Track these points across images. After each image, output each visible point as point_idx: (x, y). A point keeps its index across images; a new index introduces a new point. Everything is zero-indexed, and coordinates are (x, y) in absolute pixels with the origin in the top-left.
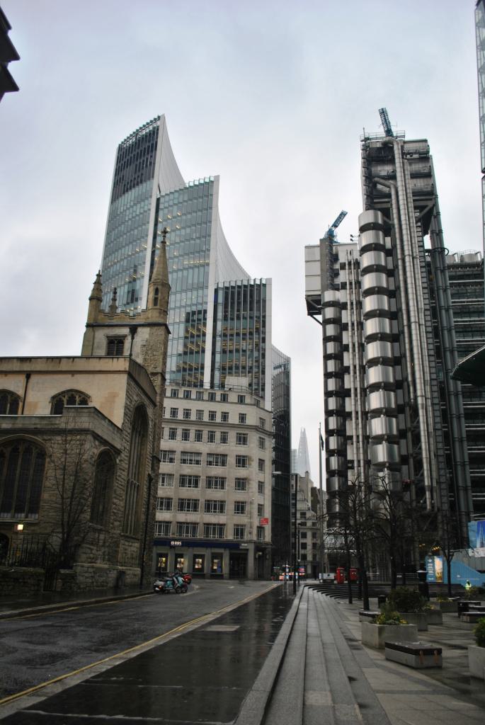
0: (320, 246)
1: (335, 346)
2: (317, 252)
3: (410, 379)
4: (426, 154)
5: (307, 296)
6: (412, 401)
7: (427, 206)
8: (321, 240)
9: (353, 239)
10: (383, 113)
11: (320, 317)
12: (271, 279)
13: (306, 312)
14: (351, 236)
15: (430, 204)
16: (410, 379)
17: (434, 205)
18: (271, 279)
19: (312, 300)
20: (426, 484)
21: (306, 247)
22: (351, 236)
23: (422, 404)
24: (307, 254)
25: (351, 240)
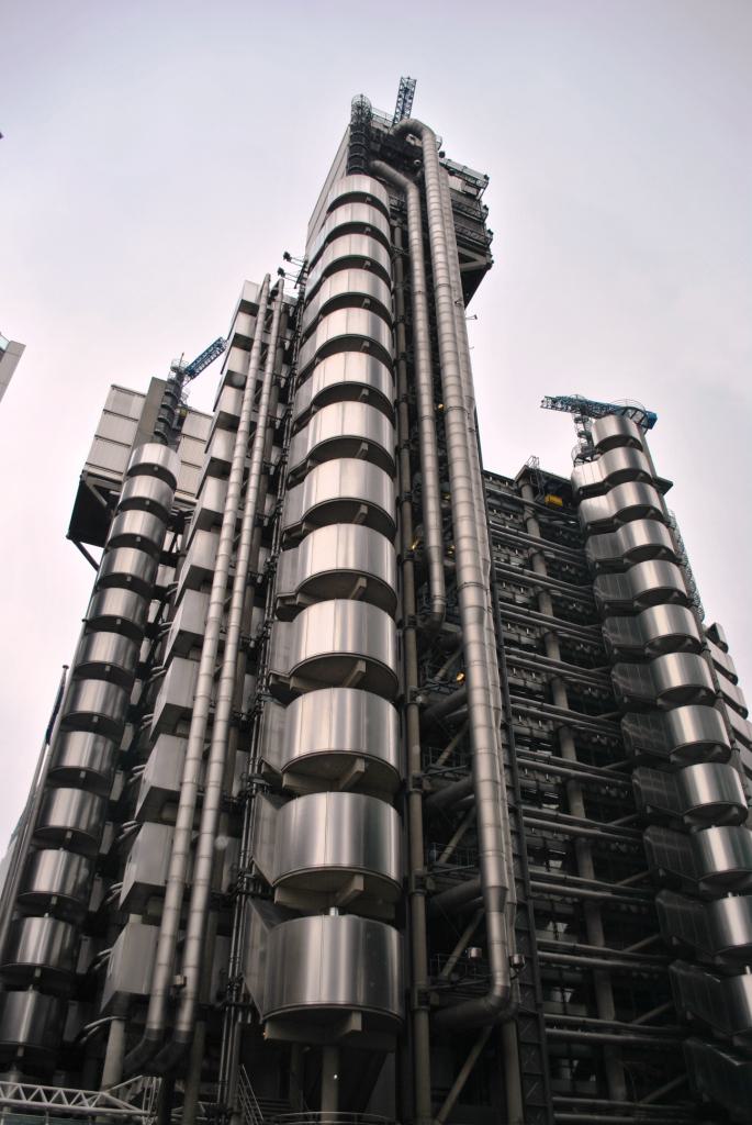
1: (140, 558)
3: (434, 539)
4: (479, 188)
5: (86, 475)
7: (475, 260)
8: (154, 380)
9: (288, 267)
10: (406, 92)
11: (97, 552)
12: (22, 347)
13: (66, 531)
14: (287, 257)
15: (481, 261)
16: (434, 539)
17: (489, 266)
18: (22, 347)
19: (96, 486)
20: (492, 878)
21: (114, 387)
22: (287, 257)
23: (481, 609)
24: (115, 400)
25: (281, 272)
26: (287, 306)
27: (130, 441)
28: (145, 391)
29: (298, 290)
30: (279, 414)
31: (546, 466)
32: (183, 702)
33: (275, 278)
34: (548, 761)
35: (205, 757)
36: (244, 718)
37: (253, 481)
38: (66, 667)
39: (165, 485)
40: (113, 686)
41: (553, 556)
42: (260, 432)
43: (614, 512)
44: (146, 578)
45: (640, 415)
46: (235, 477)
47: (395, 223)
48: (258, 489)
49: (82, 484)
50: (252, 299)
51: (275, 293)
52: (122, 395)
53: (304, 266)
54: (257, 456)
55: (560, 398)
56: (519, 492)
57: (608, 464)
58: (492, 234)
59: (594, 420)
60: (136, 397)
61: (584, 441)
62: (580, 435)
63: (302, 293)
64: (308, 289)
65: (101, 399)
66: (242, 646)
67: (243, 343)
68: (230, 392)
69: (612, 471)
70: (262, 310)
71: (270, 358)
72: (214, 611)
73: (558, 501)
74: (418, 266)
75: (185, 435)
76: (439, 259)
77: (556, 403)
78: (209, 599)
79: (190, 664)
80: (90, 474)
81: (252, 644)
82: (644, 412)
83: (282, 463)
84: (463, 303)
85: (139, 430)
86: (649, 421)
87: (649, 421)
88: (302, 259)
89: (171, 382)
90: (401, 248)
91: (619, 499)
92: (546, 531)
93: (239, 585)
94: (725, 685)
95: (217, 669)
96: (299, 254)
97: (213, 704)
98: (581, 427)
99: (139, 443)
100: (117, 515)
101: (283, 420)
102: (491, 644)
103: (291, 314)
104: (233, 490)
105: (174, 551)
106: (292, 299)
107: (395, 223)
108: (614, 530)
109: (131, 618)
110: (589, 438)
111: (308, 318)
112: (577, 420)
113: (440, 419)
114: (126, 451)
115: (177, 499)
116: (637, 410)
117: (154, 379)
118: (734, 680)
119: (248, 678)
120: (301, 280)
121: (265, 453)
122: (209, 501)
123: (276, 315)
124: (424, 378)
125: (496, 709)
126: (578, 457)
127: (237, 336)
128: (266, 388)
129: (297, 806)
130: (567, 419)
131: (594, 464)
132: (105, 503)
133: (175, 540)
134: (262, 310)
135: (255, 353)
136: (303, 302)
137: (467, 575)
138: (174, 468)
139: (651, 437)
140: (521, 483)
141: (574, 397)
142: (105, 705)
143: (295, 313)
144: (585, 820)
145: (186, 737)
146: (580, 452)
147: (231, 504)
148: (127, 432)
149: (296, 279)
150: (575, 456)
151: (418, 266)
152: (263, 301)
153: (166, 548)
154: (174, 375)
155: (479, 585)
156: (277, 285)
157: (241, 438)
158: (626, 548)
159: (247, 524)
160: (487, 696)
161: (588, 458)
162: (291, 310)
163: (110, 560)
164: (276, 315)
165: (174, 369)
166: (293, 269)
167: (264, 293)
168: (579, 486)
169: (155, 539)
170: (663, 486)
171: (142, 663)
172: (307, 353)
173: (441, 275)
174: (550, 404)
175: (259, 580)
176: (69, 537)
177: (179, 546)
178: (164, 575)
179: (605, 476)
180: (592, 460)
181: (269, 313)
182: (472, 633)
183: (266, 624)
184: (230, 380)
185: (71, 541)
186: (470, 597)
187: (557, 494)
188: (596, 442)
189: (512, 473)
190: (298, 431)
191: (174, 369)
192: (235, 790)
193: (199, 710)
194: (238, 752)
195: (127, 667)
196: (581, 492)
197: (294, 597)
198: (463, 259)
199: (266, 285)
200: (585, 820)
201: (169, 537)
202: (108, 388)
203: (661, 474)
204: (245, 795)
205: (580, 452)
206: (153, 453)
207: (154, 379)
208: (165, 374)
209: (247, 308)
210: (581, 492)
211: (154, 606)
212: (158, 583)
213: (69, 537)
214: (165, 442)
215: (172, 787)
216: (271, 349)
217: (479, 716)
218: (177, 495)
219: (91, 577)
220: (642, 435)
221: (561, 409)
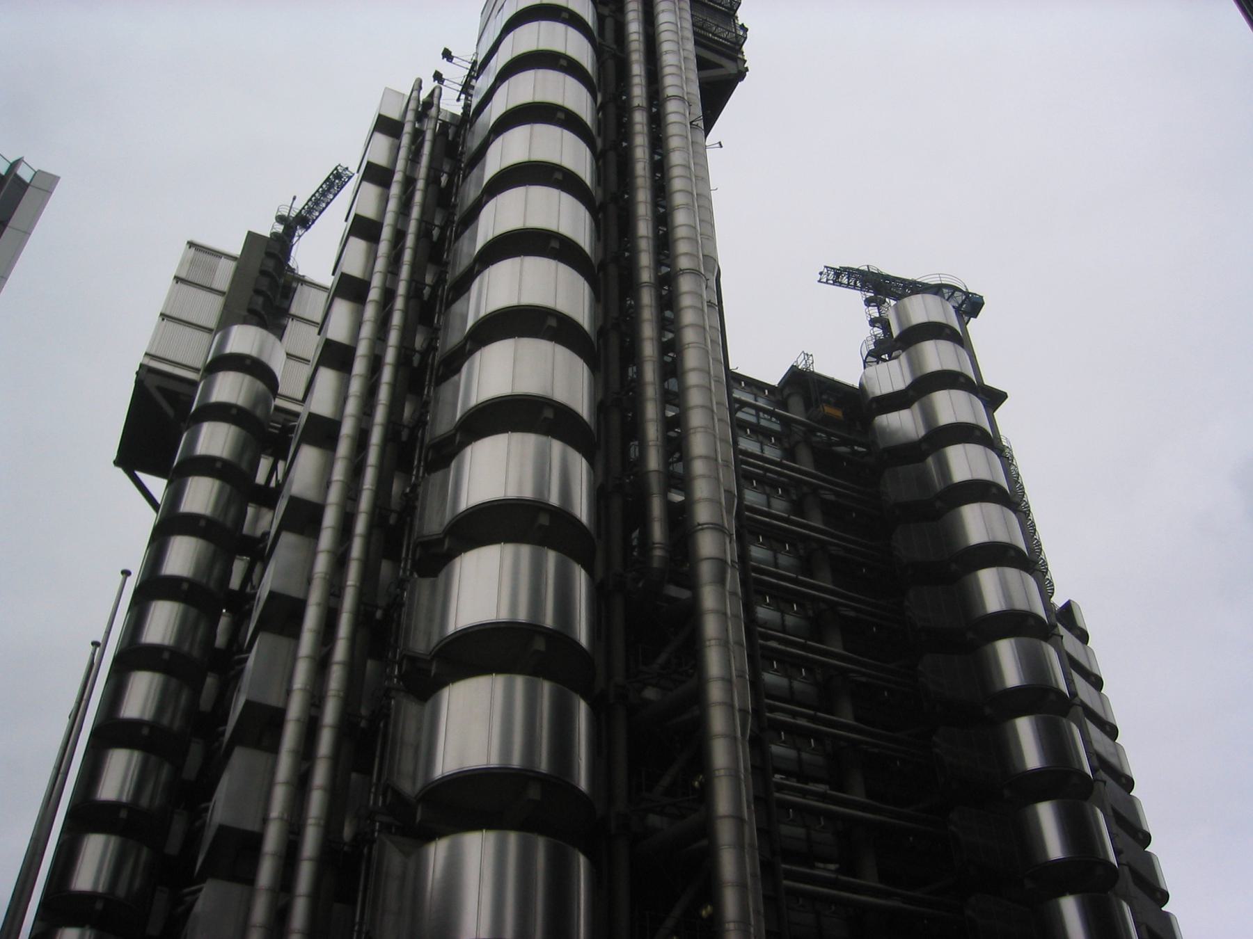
0: (242, 262)
2: (223, 275)
6: (658, 553)
7: (721, 66)
8: (252, 238)
11: (158, 486)
12: (54, 180)
13: (114, 455)
14: (447, 55)
15: (730, 68)
17: (741, 75)
18: (54, 180)
19: (159, 389)
21: (191, 244)
22: (447, 55)
23: (721, 563)
25: (438, 77)
26: (445, 125)
27: (212, 323)
28: (237, 250)
29: (462, 103)
30: (429, 279)
31: (825, 367)
32: (273, 700)
33: (429, 85)
34: (823, 797)
35: (301, 783)
36: (363, 724)
37: (387, 375)
38: (95, 644)
39: (260, 386)
40: (174, 682)
41: (832, 498)
42: (399, 303)
43: (922, 432)
44: (229, 524)
45: (959, 297)
46: (359, 367)
47: (606, 11)
48: (394, 385)
49: (139, 383)
50: (395, 114)
51: (428, 104)
52: (208, 258)
53: (472, 68)
54: (393, 337)
55: (845, 269)
56: (784, 405)
57: (914, 364)
58: (746, 30)
59: (893, 303)
60: (223, 261)
61: (878, 331)
62: (873, 322)
63: (467, 107)
64: (475, 101)
65: (173, 259)
66: (362, 617)
67: (376, 174)
68: (358, 246)
69: (919, 374)
70: (408, 128)
71: (418, 197)
72: (322, 564)
73: (838, 413)
74: (637, 69)
75: (294, 317)
76: (669, 60)
77: (841, 276)
78: (316, 544)
79: (284, 642)
80: (151, 370)
81: (379, 614)
82: (967, 294)
83: (431, 348)
84: (701, 124)
85: (226, 307)
86: (971, 306)
87: (971, 306)
88: (469, 59)
89: (275, 235)
90: (614, 46)
91: (928, 415)
92: (823, 458)
93: (360, 526)
94: (1084, 690)
95: (325, 650)
96: (467, 50)
97: (316, 700)
98: (874, 312)
99: (226, 321)
100: (188, 428)
101: (434, 288)
102: (736, 616)
103: (450, 138)
104: (356, 386)
105: (273, 484)
106: (453, 115)
107: (606, 11)
108: (922, 458)
109: (204, 581)
110: (885, 325)
111: (474, 143)
112: (868, 302)
113: (667, 284)
114: (206, 336)
115: (278, 409)
116: (955, 289)
117: (250, 234)
118: (1097, 683)
119: (370, 665)
120: (467, 88)
121: (407, 333)
122: (322, 403)
123: (429, 136)
124: (644, 228)
125: (743, 711)
126: (870, 354)
127: (369, 165)
128: (410, 241)
129: (438, 852)
130: (855, 298)
131: (895, 362)
132: (170, 412)
133: (274, 469)
134: (408, 128)
135: (395, 190)
136: (469, 118)
137: (703, 514)
138: (278, 364)
139: (975, 327)
140: (787, 392)
141: (865, 268)
142: (160, 708)
143: (457, 134)
144: (880, 886)
145: (274, 749)
146: (872, 347)
147: (352, 407)
148: (208, 309)
149: (460, 88)
150: (865, 354)
151: (637, 69)
152: (410, 116)
153: (260, 478)
154: (280, 228)
155: (718, 528)
156: (432, 95)
157: (370, 312)
158: (938, 485)
159: (376, 437)
160: (729, 690)
161: (885, 357)
162: (451, 131)
163: (175, 494)
164: (429, 136)
165: (281, 219)
166: (456, 74)
167: (412, 105)
168: (871, 396)
169: (244, 466)
170: (993, 399)
171: (218, 650)
172: (471, 192)
173: (671, 84)
174: (831, 276)
175: (392, 520)
176: (119, 462)
177: (280, 477)
178: (256, 519)
179: (909, 381)
180: (891, 358)
181: (418, 135)
182: (709, 598)
183: (401, 584)
184: (363, 228)
185: (120, 472)
186: (707, 545)
187: (837, 405)
188: (896, 331)
189: (773, 376)
190: (454, 300)
191: (281, 219)
192: (347, 833)
193: (295, 709)
194: (354, 776)
195: (196, 653)
196: (874, 406)
197: (440, 542)
198: (702, 64)
199: (415, 94)
200: (880, 886)
201: (265, 464)
202: (184, 245)
203: (991, 379)
204: (363, 839)
205: (872, 347)
206: (244, 339)
207: (250, 234)
208: (267, 227)
209: (385, 125)
210: (874, 406)
211: (239, 567)
212: (246, 529)
213: (119, 462)
214: (262, 323)
215: (251, 825)
216: (420, 184)
217: (718, 721)
218: (279, 402)
219: (150, 518)
220: (964, 325)
221: (848, 286)
